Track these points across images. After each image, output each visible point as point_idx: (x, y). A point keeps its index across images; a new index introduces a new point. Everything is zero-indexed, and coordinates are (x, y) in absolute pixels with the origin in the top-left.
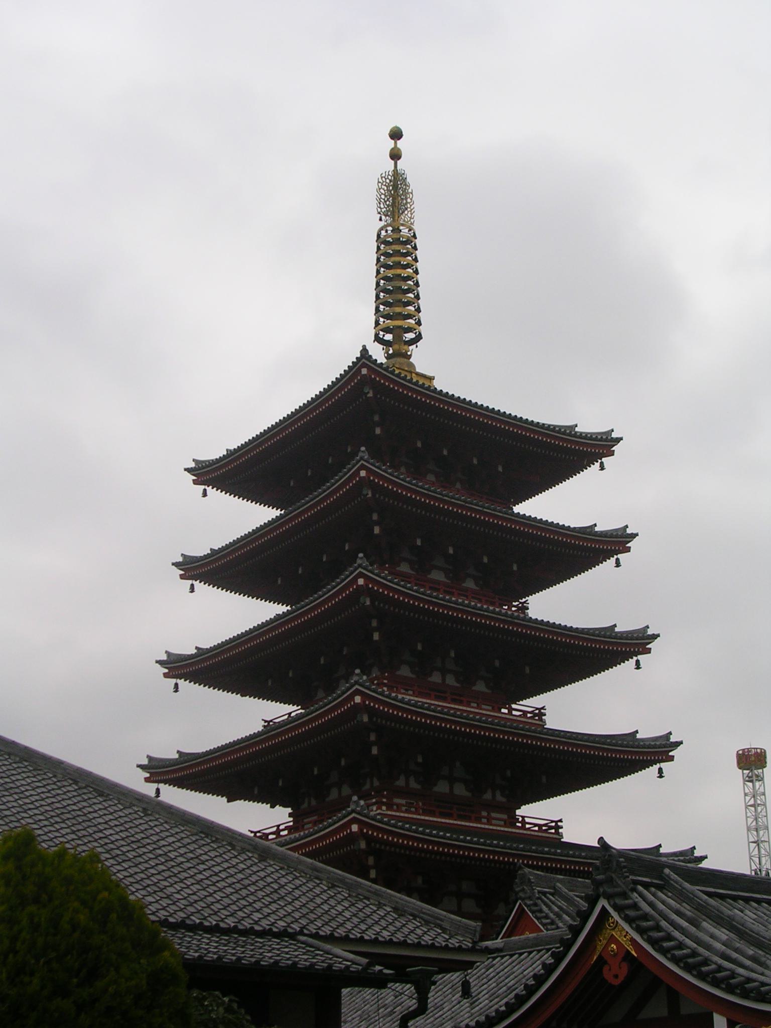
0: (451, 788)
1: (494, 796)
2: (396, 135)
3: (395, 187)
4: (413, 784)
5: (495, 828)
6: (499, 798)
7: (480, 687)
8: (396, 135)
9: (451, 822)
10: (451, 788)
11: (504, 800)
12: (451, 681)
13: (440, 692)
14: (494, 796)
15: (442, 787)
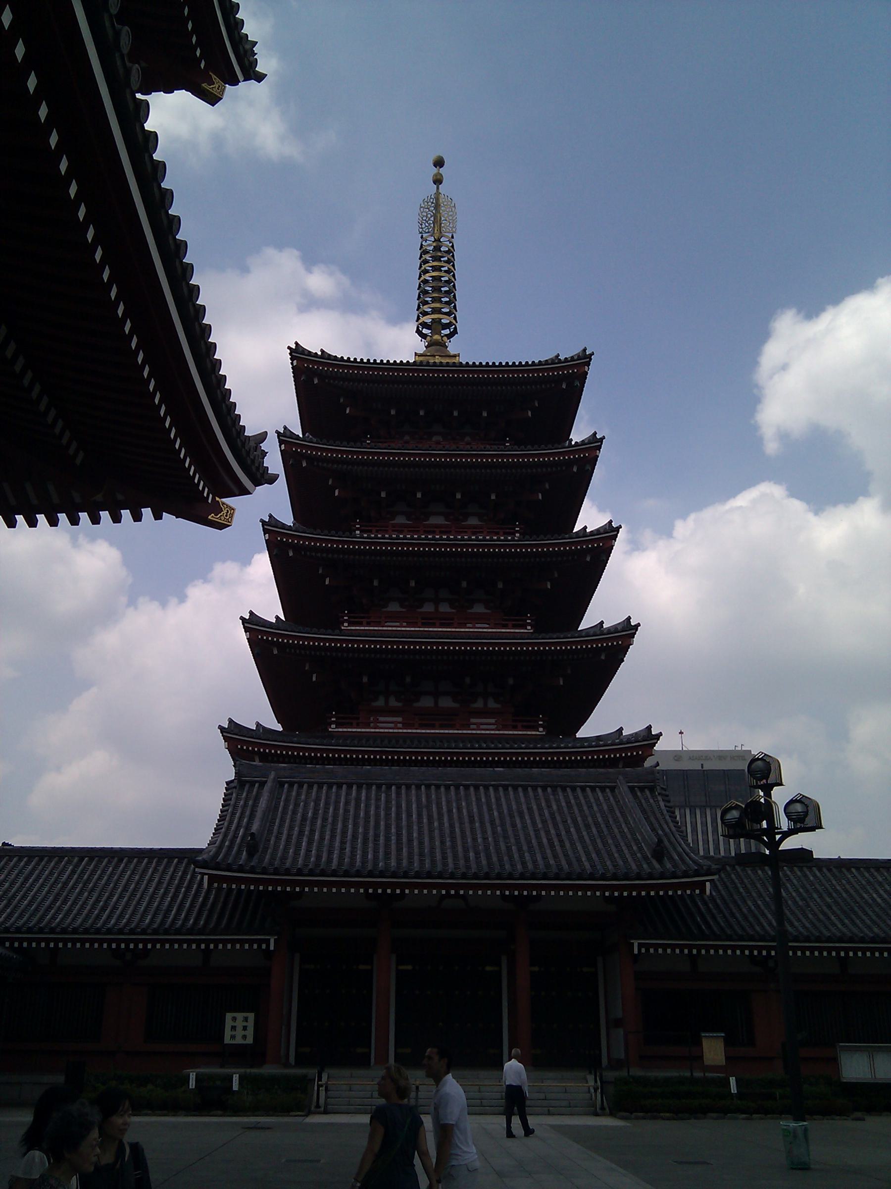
0: (436, 703)
1: (485, 704)
2: (439, 163)
3: (437, 206)
4: (393, 703)
5: (483, 732)
6: (492, 704)
7: (479, 609)
8: (439, 163)
9: (456, 732)
10: (436, 703)
11: (498, 706)
12: (444, 608)
13: (428, 620)
14: (485, 704)
15: (426, 702)
